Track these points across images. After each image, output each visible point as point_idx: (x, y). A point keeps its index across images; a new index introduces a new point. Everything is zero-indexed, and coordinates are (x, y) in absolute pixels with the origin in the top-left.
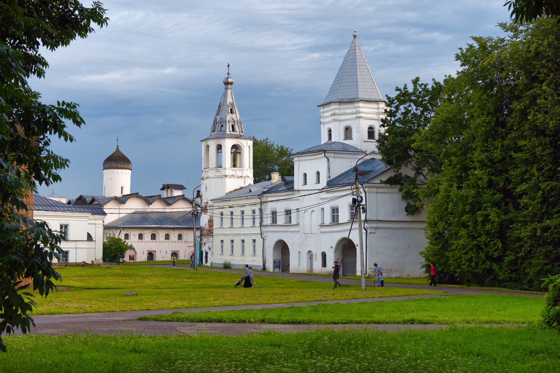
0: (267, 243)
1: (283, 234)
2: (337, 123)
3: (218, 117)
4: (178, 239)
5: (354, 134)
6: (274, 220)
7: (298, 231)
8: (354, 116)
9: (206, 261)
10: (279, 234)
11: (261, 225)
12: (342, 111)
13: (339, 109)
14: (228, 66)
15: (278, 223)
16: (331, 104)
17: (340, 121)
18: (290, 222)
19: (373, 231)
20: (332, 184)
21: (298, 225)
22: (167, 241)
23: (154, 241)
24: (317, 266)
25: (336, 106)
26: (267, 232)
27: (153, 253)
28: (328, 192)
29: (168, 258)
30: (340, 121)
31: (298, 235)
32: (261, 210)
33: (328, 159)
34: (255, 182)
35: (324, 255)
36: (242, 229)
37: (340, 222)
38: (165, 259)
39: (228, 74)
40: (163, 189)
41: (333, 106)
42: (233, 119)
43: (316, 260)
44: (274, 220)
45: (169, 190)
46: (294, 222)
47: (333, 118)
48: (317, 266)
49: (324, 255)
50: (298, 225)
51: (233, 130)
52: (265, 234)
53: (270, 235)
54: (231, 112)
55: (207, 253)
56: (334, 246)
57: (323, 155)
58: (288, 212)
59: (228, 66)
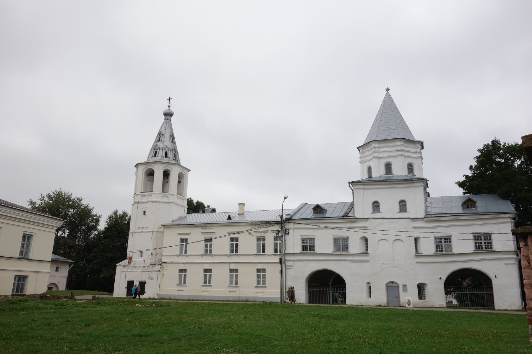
1: (331, 263)
6: (308, 247)
7: (368, 261)
12: (406, 149)
13: (404, 146)
14: (170, 99)
16: (371, 143)
17: (380, 158)
18: (347, 251)
24: (409, 298)
25: (376, 145)
30: (405, 157)
31: (366, 265)
34: (188, 213)
35: (421, 288)
39: (169, 107)
41: (398, 143)
44: (308, 247)
49: (421, 288)
53: (296, 263)
56: (444, 278)
59: (170, 99)
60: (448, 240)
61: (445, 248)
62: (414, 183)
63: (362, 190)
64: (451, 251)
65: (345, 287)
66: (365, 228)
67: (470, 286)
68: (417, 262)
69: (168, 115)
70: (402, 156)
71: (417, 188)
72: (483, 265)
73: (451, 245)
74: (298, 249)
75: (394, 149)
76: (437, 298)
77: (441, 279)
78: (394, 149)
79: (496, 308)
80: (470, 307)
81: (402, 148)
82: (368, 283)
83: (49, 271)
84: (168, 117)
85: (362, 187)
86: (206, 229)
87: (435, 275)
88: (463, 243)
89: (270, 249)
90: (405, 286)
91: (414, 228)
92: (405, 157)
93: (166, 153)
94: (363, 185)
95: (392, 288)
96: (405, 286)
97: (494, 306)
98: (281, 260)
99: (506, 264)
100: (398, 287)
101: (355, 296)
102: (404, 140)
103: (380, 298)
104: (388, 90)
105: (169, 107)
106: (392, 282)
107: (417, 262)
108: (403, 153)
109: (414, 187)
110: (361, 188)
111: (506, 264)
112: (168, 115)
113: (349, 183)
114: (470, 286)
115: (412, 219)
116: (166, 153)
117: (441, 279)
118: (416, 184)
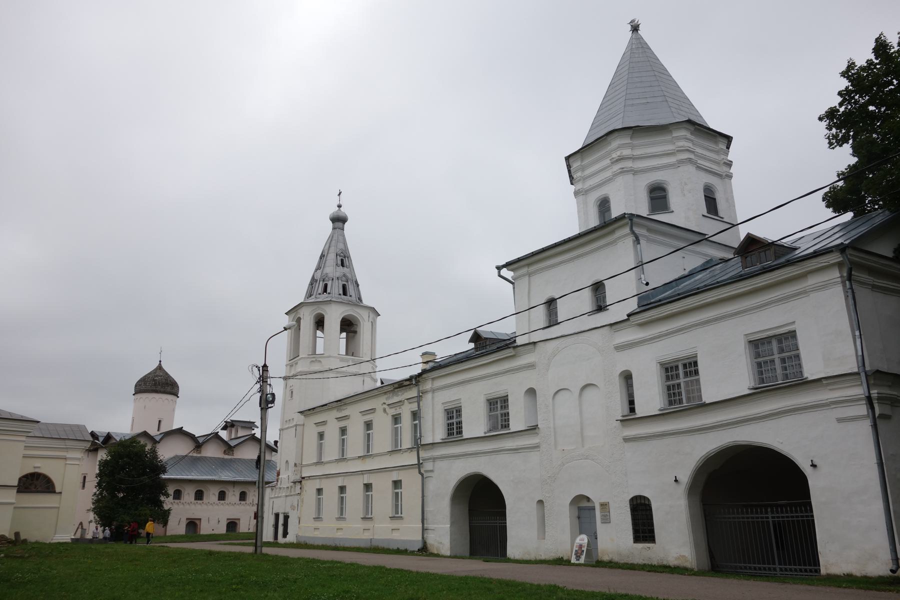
0: (431, 486)
1: (483, 459)
2: (629, 177)
3: (319, 272)
4: (240, 500)
5: (674, 199)
6: (454, 428)
7: (536, 447)
8: (672, 160)
9: (285, 534)
10: (471, 460)
11: (418, 445)
12: (638, 152)
13: (633, 147)
15: (466, 434)
18: (507, 426)
19: (887, 411)
20: (652, 303)
21: (534, 429)
22: (222, 502)
23: (199, 502)
26: (434, 459)
27: (197, 522)
28: (642, 325)
29: (222, 529)
30: (635, 172)
31: (534, 456)
32: (415, 415)
33: (637, 240)
36: (368, 460)
37: (707, 398)
38: (216, 532)
39: (340, 206)
40: (224, 428)
41: (616, 142)
42: (344, 275)
43: (606, 519)
44: (454, 428)
45: (234, 430)
46: (517, 423)
47: (616, 168)
48: (616, 537)
50: (534, 429)
51: (345, 293)
52: (428, 466)
53: (440, 464)
54: (343, 265)
55: (286, 518)
56: (685, 477)
57: (627, 230)
58: (498, 406)
60: (691, 366)
61: (688, 392)
62: (613, 232)
63: (527, 278)
64: (700, 397)
65: (503, 515)
66: (531, 366)
67: (754, 502)
68: (627, 440)
69: (339, 220)
70: (623, 172)
71: (620, 244)
72: (785, 432)
73: (698, 381)
74: (440, 434)
75: (607, 162)
76: (677, 538)
77: (676, 481)
78: (607, 162)
79: (823, 571)
80: (777, 566)
81: (627, 152)
82: (541, 502)
83: (13, 501)
84: (340, 224)
85: (524, 271)
86: (341, 410)
87: (666, 470)
88: (726, 373)
89: (407, 441)
90: (604, 506)
91: (620, 348)
92: (635, 172)
93: (326, 286)
94: (529, 265)
95: (584, 511)
96: (604, 506)
97: (816, 562)
98: (258, 461)
99: (840, 420)
100: (593, 509)
101: (522, 538)
102: (630, 132)
103: (562, 539)
104: (635, 28)
105: (340, 206)
106: (588, 499)
107: (627, 440)
108: (628, 164)
109: (614, 242)
110: (524, 275)
111: (840, 420)
112: (339, 220)
113: (499, 268)
114: (754, 502)
115: (611, 325)
116: (344, 287)
117: (676, 481)
118: (619, 233)
